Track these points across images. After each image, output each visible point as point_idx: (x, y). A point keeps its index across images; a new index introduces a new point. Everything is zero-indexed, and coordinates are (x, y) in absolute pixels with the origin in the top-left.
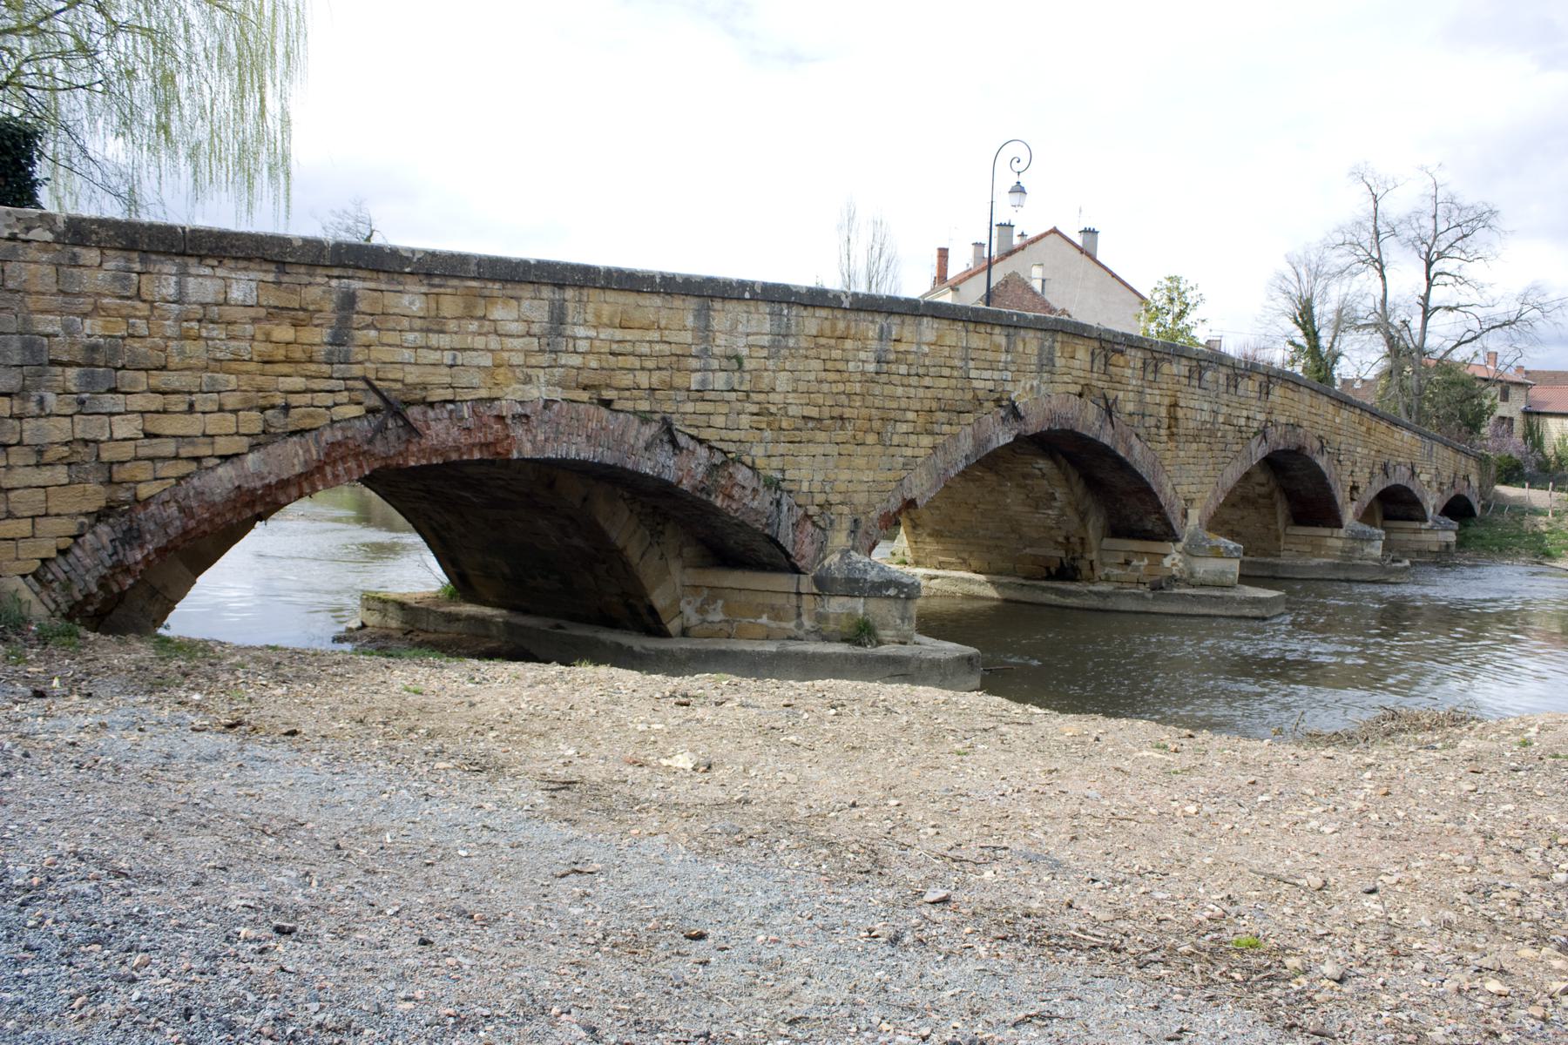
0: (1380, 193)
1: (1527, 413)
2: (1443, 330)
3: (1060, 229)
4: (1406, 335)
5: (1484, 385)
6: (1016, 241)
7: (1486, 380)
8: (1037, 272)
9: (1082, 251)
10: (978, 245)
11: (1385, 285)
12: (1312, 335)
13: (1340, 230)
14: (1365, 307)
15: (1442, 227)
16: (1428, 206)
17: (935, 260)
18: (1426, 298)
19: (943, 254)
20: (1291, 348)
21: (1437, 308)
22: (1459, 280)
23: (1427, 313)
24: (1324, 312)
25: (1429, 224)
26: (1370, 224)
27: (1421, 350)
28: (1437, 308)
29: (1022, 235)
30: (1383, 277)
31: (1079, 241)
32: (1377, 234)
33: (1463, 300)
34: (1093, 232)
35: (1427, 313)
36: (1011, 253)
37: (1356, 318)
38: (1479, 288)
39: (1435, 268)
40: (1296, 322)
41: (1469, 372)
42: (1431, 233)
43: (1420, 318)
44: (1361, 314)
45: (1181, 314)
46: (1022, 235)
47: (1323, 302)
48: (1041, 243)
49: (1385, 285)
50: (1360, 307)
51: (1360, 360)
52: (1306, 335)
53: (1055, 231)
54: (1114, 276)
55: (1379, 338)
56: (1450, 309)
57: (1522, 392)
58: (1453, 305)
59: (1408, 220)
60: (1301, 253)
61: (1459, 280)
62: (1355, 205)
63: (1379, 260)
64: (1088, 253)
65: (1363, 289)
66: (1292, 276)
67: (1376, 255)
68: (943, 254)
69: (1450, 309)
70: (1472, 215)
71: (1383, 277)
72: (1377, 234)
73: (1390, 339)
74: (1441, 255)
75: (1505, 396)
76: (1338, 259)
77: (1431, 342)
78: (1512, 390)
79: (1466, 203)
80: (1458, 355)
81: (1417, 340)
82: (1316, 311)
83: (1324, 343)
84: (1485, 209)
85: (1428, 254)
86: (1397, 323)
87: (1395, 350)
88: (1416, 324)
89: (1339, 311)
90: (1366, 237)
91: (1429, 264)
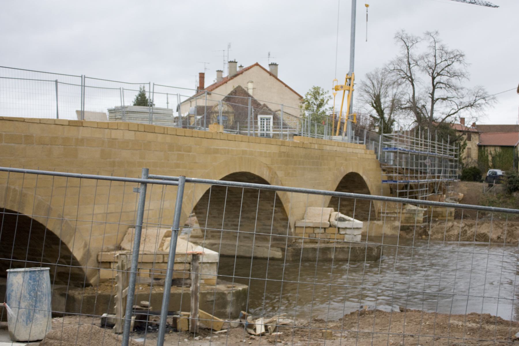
0: (410, 44)
1: (480, 146)
2: (442, 110)
3: (259, 63)
4: (424, 112)
5: (461, 134)
6: (238, 69)
7: (460, 131)
8: (250, 86)
9: (271, 74)
10: (220, 72)
11: (414, 88)
12: (381, 112)
13: (392, 63)
14: (405, 100)
15: (438, 62)
16: (431, 51)
17: (198, 79)
18: (432, 94)
19: (202, 76)
20: (372, 119)
21: (437, 99)
22: (448, 86)
23: (433, 102)
24: (386, 102)
25: (432, 59)
26: (406, 60)
27: (431, 118)
28: (437, 99)
29: (241, 66)
30: (413, 85)
31: (268, 69)
32: (409, 64)
33: (449, 95)
34: (276, 65)
35: (433, 102)
36: (236, 76)
37: (401, 105)
38: (456, 89)
39: (437, 79)
40: (373, 106)
41: (454, 128)
42: (434, 64)
43: (431, 104)
44: (403, 103)
45: (320, 105)
46: (241, 66)
47: (385, 97)
48: (251, 70)
49: (414, 88)
50: (403, 99)
51: (404, 122)
52: (378, 112)
53: (257, 64)
54: (286, 86)
55: (412, 114)
56: (444, 99)
57: (477, 137)
58: (445, 97)
59: (422, 58)
60: (373, 73)
61: (448, 86)
62: (397, 52)
63: (411, 77)
64: (273, 75)
65: (405, 93)
66: (369, 83)
67: (409, 75)
68: (202, 76)
69: (444, 99)
70: (452, 56)
71: (413, 85)
72: (409, 64)
73: (418, 114)
74: (439, 74)
75: (469, 139)
76: (391, 77)
77: (436, 115)
78: (472, 136)
79: (449, 50)
80: (449, 120)
81: (429, 115)
82: (382, 100)
83: (386, 116)
84: (458, 53)
85: (433, 74)
86: (420, 106)
87: (420, 119)
88: (429, 107)
89: (393, 101)
90: (404, 67)
91: (433, 78)
